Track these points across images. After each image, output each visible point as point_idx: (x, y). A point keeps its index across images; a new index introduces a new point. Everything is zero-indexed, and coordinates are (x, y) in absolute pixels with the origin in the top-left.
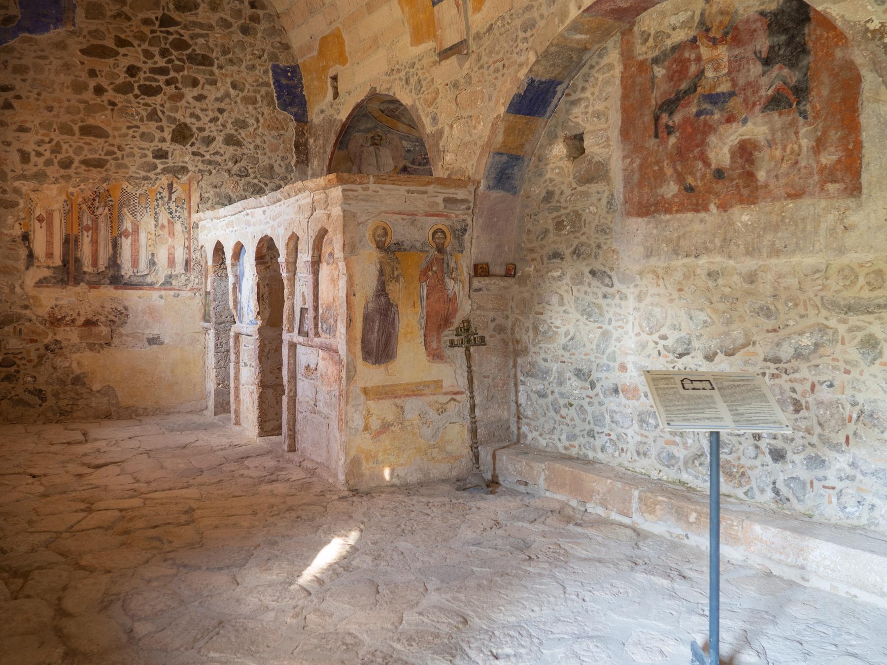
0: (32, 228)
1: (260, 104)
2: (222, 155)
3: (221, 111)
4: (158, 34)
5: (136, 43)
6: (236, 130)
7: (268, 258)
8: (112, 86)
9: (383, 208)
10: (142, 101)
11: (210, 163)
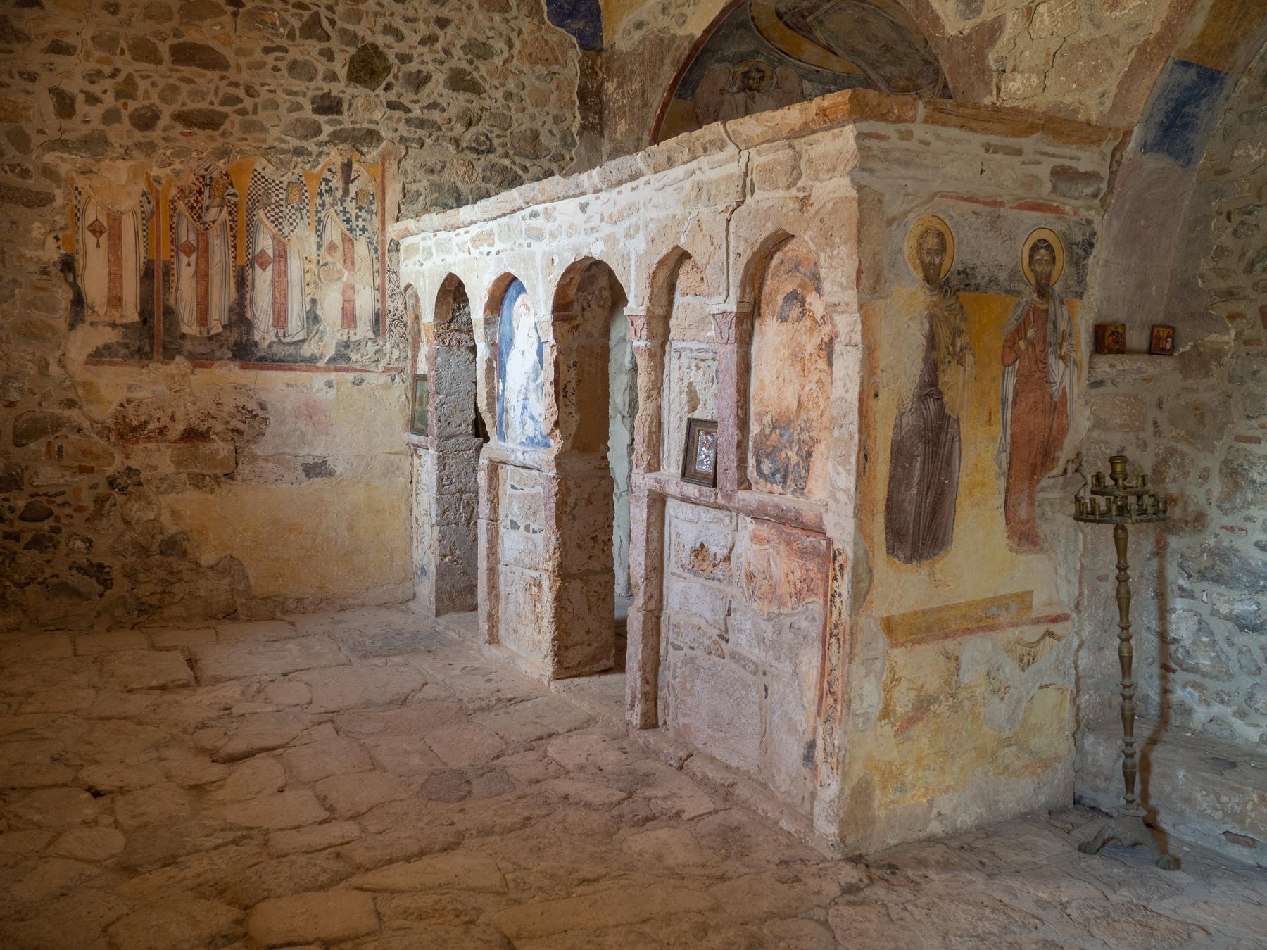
0: (80, 247)
1: (514, 12)
2: (443, 110)
3: (442, 23)
6: (471, 62)
7: (576, 308)
9: (937, 186)
11: (421, 124)
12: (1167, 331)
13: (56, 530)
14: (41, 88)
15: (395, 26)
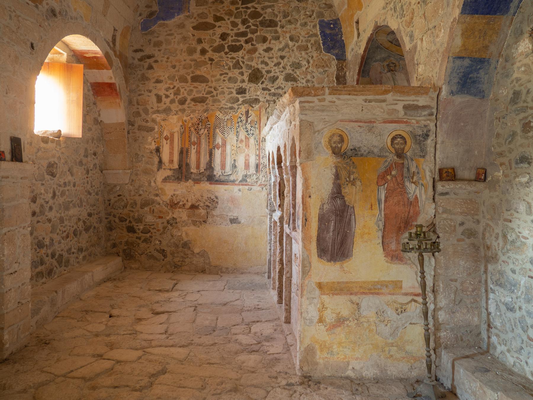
0: (161, 144)
1: (310, 50)
2: (283, 89)
3: (282, 58)
4: (241, 9)
5: (226, 18)
6: (293, 70)
8: (211, 48)
9: (340, 117)
10: (230, 56)
11: (274, 95)
12: (482, 170)
13: (151, 237)
14: (152, 95)
15: (265, 61)
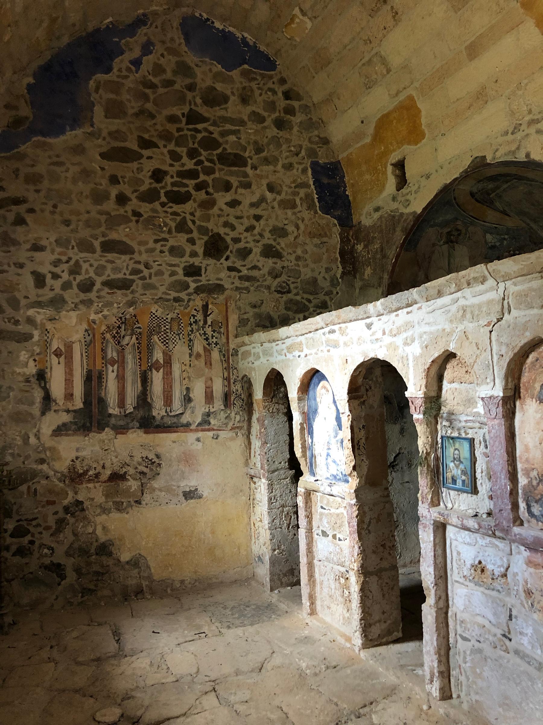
1: (299, 208)
2: (260, 269)
3: (258, 218)
4: (186, 132)
5: (161, 143)
6: (275, 240)
8: (136, 194)
10: (170, 210)
11: (248, 278)
13: (32, 542)
15: (230, 221)
